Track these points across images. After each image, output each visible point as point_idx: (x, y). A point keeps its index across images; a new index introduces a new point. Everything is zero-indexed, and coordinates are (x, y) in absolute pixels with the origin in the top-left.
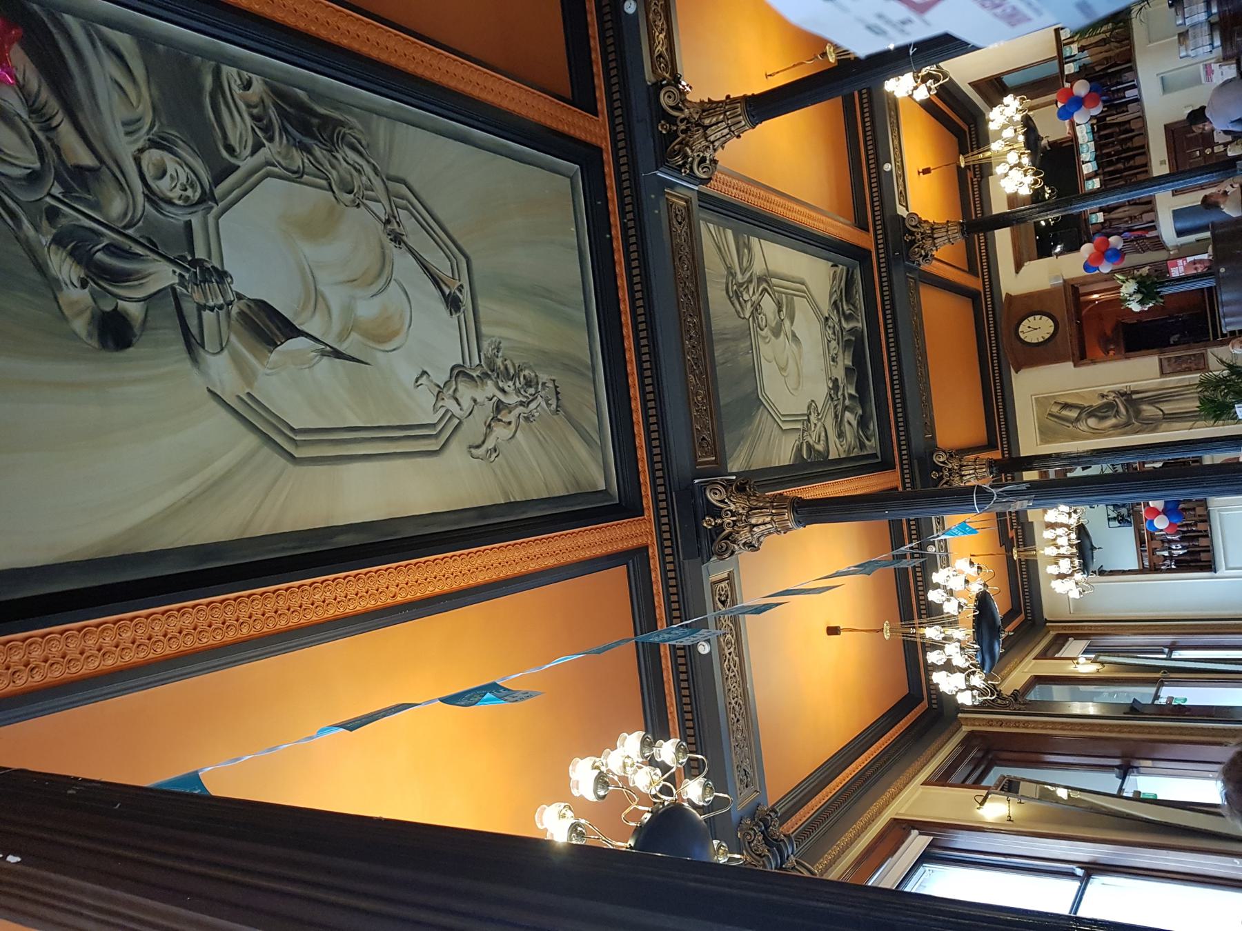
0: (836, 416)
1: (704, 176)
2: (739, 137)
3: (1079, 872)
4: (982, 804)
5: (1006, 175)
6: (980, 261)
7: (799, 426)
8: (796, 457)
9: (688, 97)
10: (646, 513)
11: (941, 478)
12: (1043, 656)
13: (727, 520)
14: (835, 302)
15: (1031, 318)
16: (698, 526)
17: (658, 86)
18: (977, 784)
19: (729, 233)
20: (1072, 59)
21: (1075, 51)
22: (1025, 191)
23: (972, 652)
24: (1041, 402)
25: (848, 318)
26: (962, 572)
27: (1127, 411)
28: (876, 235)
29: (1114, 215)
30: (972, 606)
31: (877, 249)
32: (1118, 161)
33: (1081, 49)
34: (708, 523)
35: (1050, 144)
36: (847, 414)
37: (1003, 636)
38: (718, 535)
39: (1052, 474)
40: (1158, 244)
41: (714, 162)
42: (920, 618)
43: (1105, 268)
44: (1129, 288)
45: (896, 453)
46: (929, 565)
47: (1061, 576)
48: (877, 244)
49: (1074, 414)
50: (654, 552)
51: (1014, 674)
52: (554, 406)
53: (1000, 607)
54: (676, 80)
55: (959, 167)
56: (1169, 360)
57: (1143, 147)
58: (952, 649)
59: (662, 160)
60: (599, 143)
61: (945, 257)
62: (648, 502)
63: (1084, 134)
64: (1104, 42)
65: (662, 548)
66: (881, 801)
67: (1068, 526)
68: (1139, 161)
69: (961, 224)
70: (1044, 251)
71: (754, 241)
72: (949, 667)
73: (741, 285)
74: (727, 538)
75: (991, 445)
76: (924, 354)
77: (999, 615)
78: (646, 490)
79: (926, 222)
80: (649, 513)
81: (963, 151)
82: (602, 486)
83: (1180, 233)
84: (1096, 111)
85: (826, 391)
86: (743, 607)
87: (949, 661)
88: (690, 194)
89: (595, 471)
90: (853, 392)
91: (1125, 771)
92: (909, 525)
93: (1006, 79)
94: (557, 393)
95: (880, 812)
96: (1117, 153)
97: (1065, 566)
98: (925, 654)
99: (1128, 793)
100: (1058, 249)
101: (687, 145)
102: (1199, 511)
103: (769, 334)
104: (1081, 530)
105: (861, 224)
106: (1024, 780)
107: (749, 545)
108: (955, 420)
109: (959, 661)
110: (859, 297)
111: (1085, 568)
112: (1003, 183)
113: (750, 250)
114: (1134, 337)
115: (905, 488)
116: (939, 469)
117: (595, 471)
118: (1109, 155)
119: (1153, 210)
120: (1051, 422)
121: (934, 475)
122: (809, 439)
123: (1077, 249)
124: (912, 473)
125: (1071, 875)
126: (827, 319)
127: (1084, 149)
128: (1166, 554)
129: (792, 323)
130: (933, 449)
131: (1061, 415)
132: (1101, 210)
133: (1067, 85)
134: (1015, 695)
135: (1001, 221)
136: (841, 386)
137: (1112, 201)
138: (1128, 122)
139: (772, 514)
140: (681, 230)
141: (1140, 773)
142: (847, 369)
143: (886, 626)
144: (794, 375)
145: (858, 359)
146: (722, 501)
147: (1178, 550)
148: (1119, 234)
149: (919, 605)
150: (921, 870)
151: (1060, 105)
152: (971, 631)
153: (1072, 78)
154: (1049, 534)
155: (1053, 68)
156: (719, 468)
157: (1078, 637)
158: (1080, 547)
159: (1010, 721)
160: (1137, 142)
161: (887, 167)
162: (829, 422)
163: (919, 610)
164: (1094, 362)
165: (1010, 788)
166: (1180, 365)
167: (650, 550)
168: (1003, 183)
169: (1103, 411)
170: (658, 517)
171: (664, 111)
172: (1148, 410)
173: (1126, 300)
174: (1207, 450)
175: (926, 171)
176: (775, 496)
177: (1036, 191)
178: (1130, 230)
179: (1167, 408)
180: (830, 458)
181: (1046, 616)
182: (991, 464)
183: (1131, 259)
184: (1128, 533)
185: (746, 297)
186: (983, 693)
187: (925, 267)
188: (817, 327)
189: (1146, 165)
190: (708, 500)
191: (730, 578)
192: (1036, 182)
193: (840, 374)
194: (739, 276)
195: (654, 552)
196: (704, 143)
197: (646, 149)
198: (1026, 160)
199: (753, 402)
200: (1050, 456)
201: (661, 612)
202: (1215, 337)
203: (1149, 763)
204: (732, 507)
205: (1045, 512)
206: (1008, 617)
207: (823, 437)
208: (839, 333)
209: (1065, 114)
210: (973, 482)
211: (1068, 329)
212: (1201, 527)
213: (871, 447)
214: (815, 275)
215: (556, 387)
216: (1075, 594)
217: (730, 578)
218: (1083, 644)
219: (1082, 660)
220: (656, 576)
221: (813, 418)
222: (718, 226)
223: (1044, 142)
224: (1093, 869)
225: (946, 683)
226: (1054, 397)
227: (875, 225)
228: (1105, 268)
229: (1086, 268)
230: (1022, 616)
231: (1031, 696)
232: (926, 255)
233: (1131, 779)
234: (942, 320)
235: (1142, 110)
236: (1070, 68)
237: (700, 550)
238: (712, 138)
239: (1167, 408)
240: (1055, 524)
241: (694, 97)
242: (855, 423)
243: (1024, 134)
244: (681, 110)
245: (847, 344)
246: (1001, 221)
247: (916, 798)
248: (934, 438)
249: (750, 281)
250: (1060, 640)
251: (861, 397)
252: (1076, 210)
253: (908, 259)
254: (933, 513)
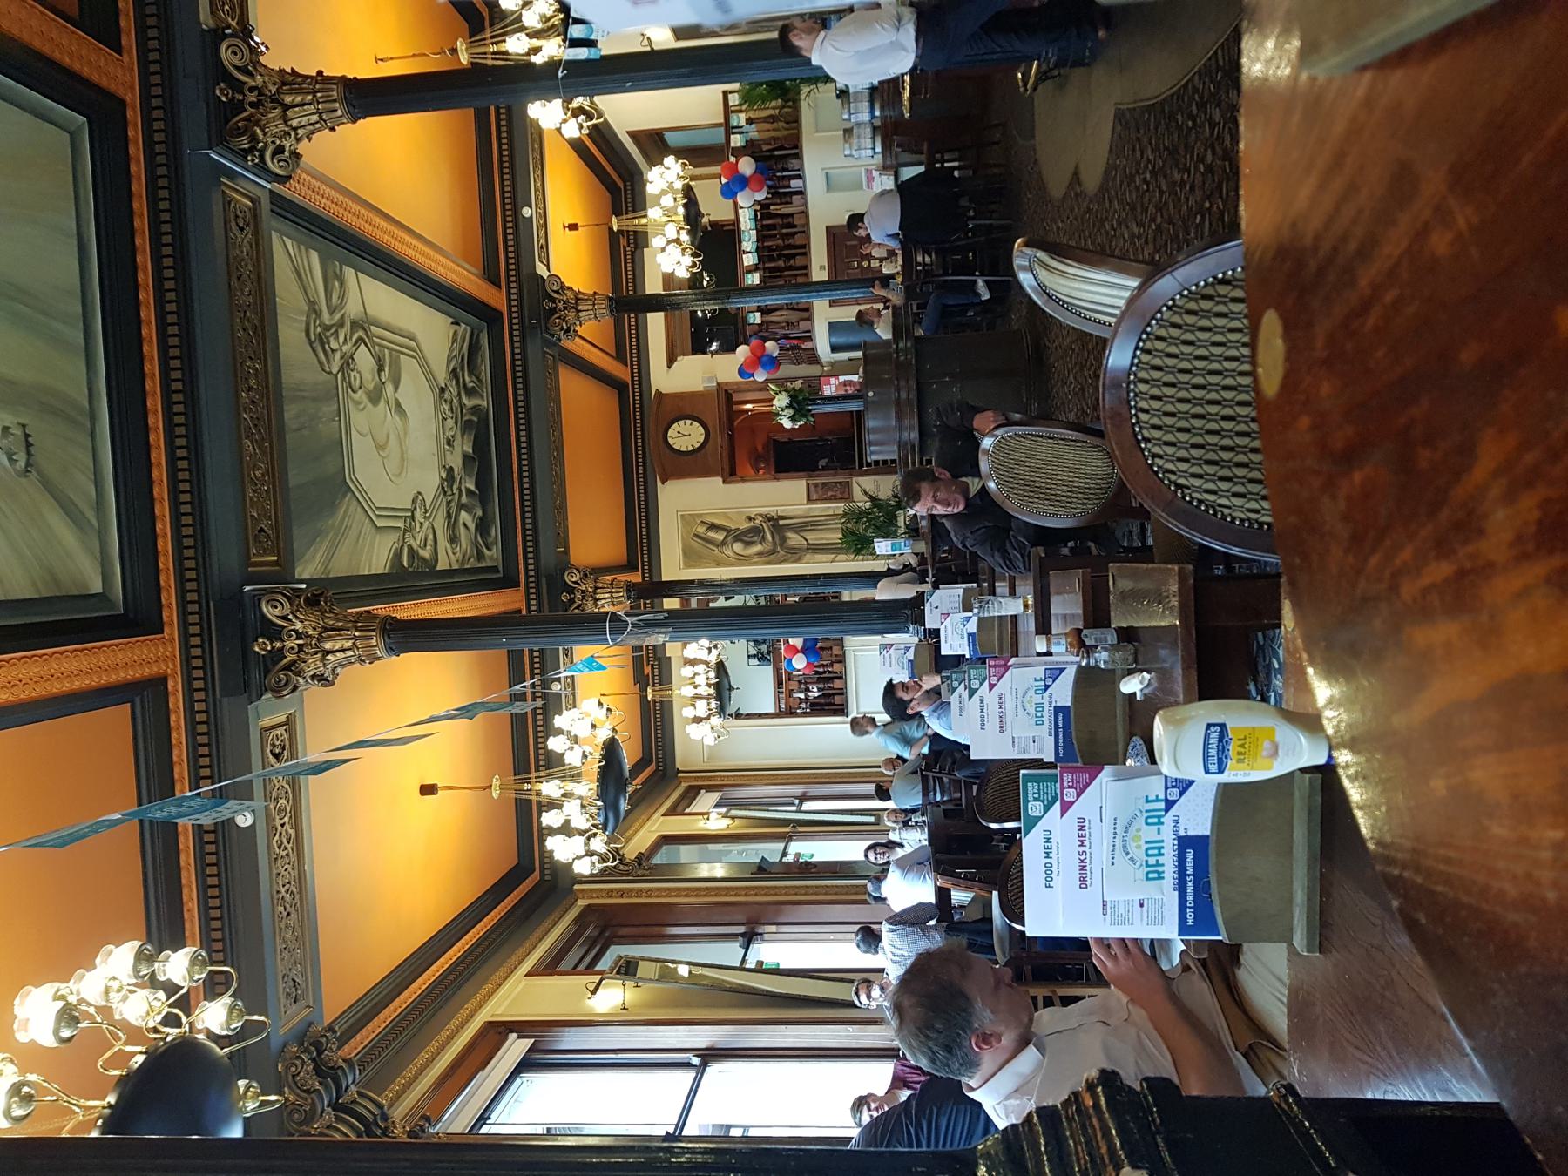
0: (449, 516)
1: (280, 172)
2: (333, 129)
3: (696, 1061)
4: (594, 993)
5: (663, 250)
6: (629, 347)
7: (400, 524)
8: (392, 567)
9: (262, 59)
10: (167, 630)
11: (572, 601)
12: (672, 812)
13: (289, 644)
14: (454, 370)
16: (246, 652)
17: (217, 35)
18: (589, 970)
19: (314, 256)
20: (738, 130)
21: (743, 123)
22: (682, 273)
23: (594, 810)
24: (687, 520)
25: (471, 392)
26: (588, 715)
28: (509, 294)
29: (772, 318)
30: (597, 755)
31: (510, 312)
32: (780, 257)
33: (750, 121)
34: (261, 647)
35: (713, 224)
36: (464, 515)
37: (630, 789)
38: (275, 664)
39: (694, 605)
40: (812, 357)
41: (296, 156)
42: (537, 770)
43: (760, 376)
44: (781, 401)
45: (521, 567)
46: (551, 705)
47: (697, 720)
48: (510, 306)
49: (720, 537)
50: (176, 685)
51: (640, 834)
52: (22, 464)
53: (628, 757)
54: (246, 32)
55: (611, 229)
56: (816, 485)
57: (804, 246)
58: (572, 810)
59: (220, 138)
60: (121, 92)
61: (590, 335)
62: (170, 614)
63: (746, 221)
64: (772, 119)
65: (188, 680)
66: (474, 1002)
67: (707, 663)
68: (799, 261)
69: (610, 299)
70: (699, 348)
71: (349, 273)
72: (566, 830)
73: (327, 328)
74: (288, 667)
75: (631, 566)
76: (560, 448)
77: (627, 765)
78: (169, 597)
79: (570, 288)
80: (172, 631)
81: (617, 213)
82: (96, 587)
83: (835, 348)
84: (761, 196)
85: (438, 481)
86: (305, 764)
87: (567, 822)
88: (258, 192)
89: (87, 564)
90: (472, 487)
91: (749, 939)
92: (532, 657)
93: (667, 136)
94: (29, 445)
95: (471, 1016)
96: (779, 248)
97: (702, 708)
98: (539, 816)
99: (751, 965)
100: (714, 347)
101: (257, 123)
102: (836, 651)
103: (365, 399)
104: (720, 668)
105: (491, 277)
106: (643, 959)
107: (320, 679)
108: (593, 534)
109: (580, 822)
110: (485, 368)
111: (721, 710)
112: (660, 258)
113: (342, 284)
114: (787, 458)
115: (529, 611)
116: (571, 590)
117: (87, 564)
118: (770, 249)
119: (810, 319)
120: (696, 544)
121: (565, 597)
122: (412, 542)
123: (734, 350)
124: (538, 594)
125: (687, 1065)
126: (442, 390)
127: (745, 236)
128: (802, 696)
129: (396, 388)
130: (565, 565)
131: (709, 536)
132: (759, 309)
133: (732, 159)
134: (640, 859)
135: (655, 303)
136: (457, 478)
137: (770, 301)
138: (791, 215)
139: (355, 638)
140: (244, 239)
141: (763, 940)
142: (466, 457)
143: (496, 783)
144: (397, 458)
145: (480, 445)
146: (285, 618)
147: (815, 693)
148: (776, 340)
149: (537, 755)
150: (518, 1081)
151: (724, 181)
152: (594, 785)
153: (738, 153)
154: (687, 671)
155: (718, 137)
156: (282, 573)
157: (710, 789)
158: (718, 686)
159: (631, 890)
160: (798, 240)
161: (526, 212)
162: (440, 523)
163: (537, 760)
164: (743, 480)
165: (627, 969)
167: (170, 683)
168: (660, 258)
169: (747, 536)
170: (185, 636)
171: (226, 70)
172: (794, 539)
173: (778, 414)
174: (846, 586)
175: (573, 227)
176: (359, 614)
177: (693, 274)
178: (786, 337)
179: (812, 537)
180: (439, 568)
181: (678, 766)
182: (630, 587)
183: (786, 370)
184: (768, 670)
185: (334, 345)
186: (603, 859)
187: (566, 343)
188: (429, 398)
189: (805, 267)
190: (263, 616)
191: (289, 723)
192: (694, 265)
193: (456, 462)
194: (326, 315)
195: (176, 685)
196: (282, 127)
197: (194, 120)
198: (685, 237)
199: (336, 487)
200: (692, 582)
201: (182, 770)
202: (861, 466)
203: (773, 928)
204: (299, 626)
205: (685, 646)
206: (638, 768)
207: (430, 541)
208: (457, 411)
209: (729, 192)
210: (607, 609)
211: (719, 439)
212: (837, 668)
213: (491, 558)
214: (432, 331)
215: (27, 436)
216: (710, 740)
217: (289, 723)
218: (714, 797)
219: (713, 816)
220: (178, 719)
221: (419, 515)
222: (299, 243)
223: (705, 220)
224: (710, 1055)
225: (562, 849)
227: (508, 282)
228: (760, 376)
229: (741, 372)
230: (653, 767)
231: (658, 859)
232: (568, 330)
233: (754, 947)
234: (582, 408)
235: (805, 204)
236: (737, 141)
237: (246, 685)
238: (294, 123)
239: (812, 537)
240: (693, 659)
241: (271, 60)
242: (472, 527)
243: (685, 205)
244: (251, 75)
245: (467, 426)
246: (655, 303)
247: (520, 993)
248: (566, 552)
249: (341, 324)
250: (692, 793)
251: (482, 494)
252: (734, 304)
253: (547, 329)
254: (561, 643)
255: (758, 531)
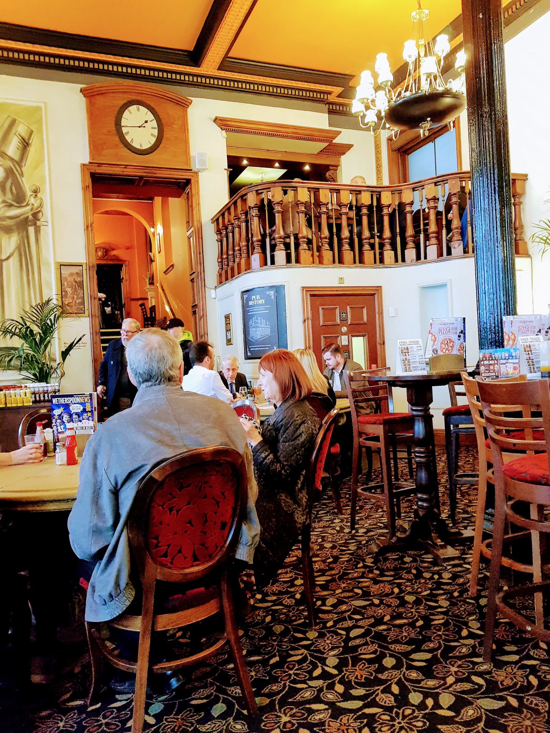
15: (155, 124)
27: (11, 218)
166: (71, 287)
226: (40, 131)
255: (20, 199)
